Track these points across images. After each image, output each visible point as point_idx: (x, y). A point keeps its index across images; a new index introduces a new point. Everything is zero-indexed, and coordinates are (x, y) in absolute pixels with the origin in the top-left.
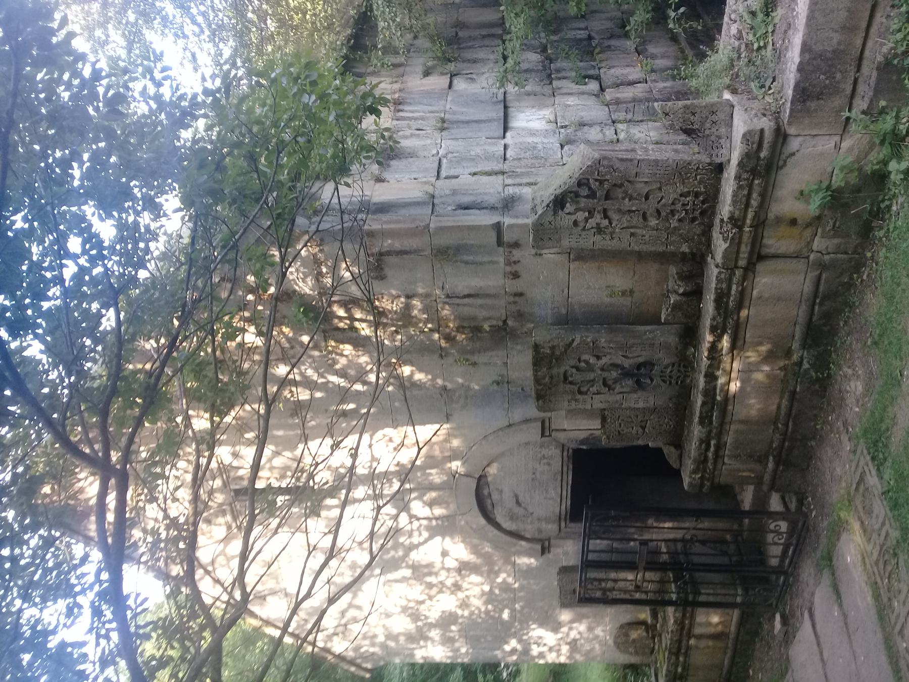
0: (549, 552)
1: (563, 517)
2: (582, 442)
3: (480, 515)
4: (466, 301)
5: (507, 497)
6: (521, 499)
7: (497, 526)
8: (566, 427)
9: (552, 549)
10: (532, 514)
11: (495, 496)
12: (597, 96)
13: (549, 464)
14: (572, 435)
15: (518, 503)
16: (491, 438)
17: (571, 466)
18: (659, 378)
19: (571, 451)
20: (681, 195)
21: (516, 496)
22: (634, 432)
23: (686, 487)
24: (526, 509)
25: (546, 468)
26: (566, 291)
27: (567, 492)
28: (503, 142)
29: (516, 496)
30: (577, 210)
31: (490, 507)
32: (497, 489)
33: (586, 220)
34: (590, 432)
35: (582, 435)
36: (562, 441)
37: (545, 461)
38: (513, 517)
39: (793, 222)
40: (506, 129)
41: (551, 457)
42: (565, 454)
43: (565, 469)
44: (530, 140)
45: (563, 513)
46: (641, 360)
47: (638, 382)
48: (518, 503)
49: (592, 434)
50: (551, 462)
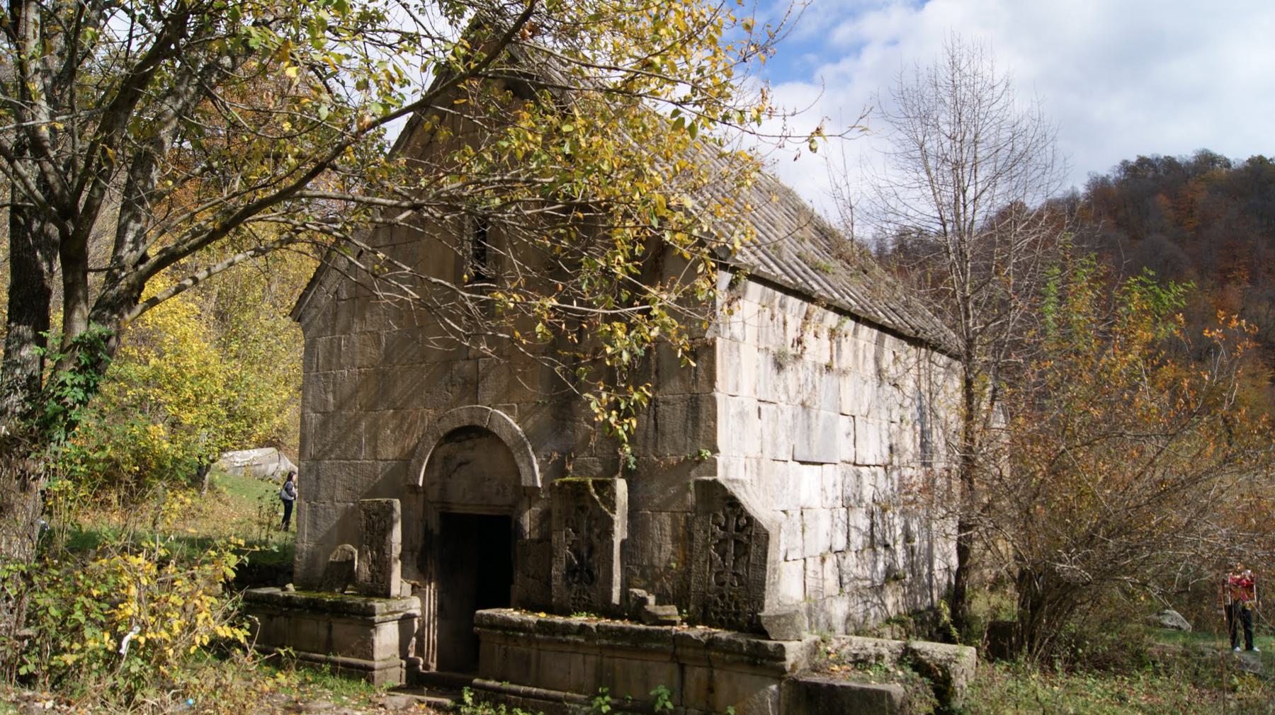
11: (468, 444)
12: (831, 548)
13: (498, 493)
15: (461, 464)
20: (737, 603)
21: (467, 463)
23: (479, 612)
27: (470, 510)
28: (789, 458)
29: (467, 463)
30: (727, 518)
33: (719, 525)
38: (447, 459)
39: (711, 690)
40: (802, 463)
44: (791, 483)
46: (595, 572)
47: (575, 570)
48: (461, 464)
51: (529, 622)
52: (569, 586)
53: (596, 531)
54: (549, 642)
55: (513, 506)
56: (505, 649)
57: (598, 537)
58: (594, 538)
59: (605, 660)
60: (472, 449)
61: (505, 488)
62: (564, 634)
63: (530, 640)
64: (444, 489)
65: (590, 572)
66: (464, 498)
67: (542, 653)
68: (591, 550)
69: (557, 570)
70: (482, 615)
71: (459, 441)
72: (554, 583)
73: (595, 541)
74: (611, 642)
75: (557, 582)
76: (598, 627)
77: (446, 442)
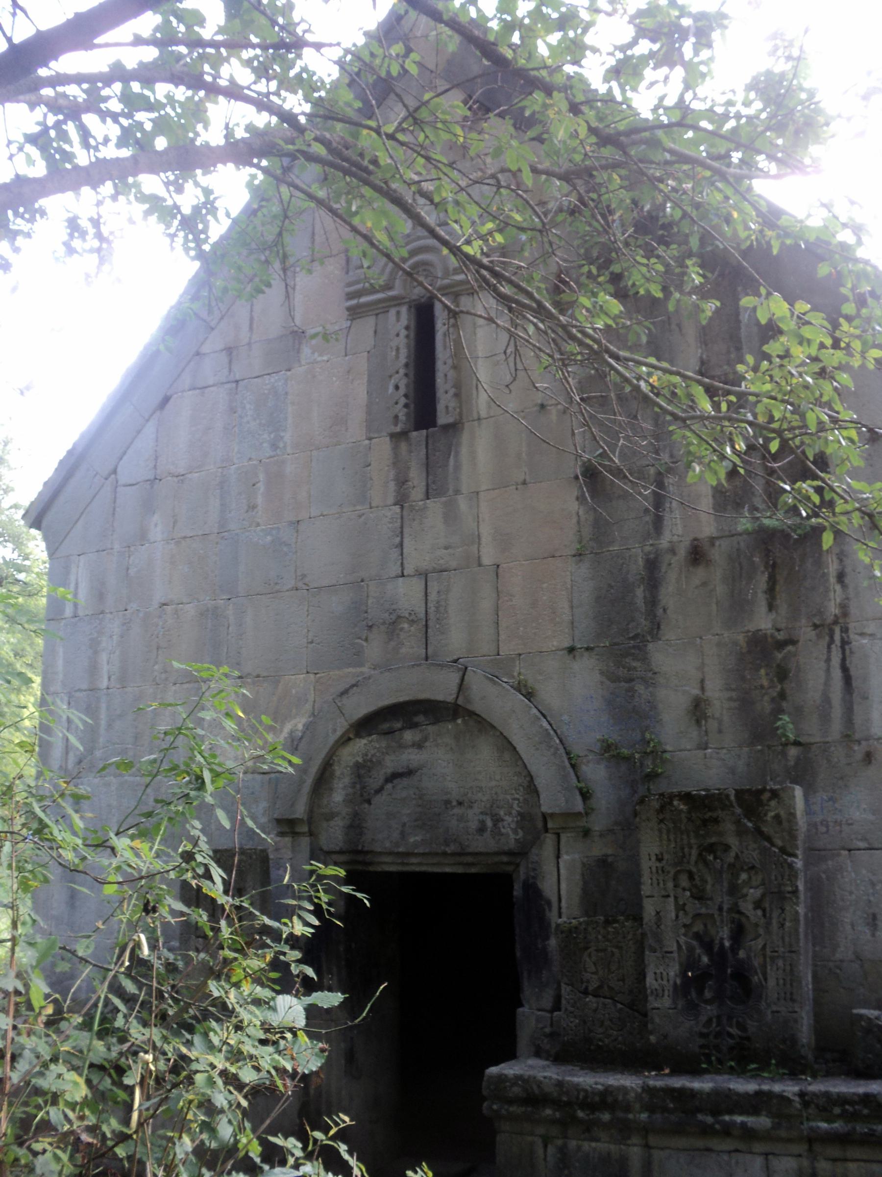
0: (282, 834)
1: (360, 858)
2: (532, 890)
3: (372, 708)
4: (837, 674)
5: (411, 757)
6: (405, 781)
7: (344, 740)
8: (565, 857)
9: (288, 840)
10: (369, 802)
11: (409, 736)
13: (482, 829)
14: (548, 867)
16: (545, 724)
17: (473, 870)
18: (715, 1012)
19: (510, 868)
22: (587, 976)
23: (493, 1070)
24: (379, 790)
25: (474, 825)
26: (862, 845)
29: (409, 773)
31: (385, 726)
32: (425, 739)
34: (554, 900)
35: (548, 887)
36: (534, 850)
37: (489, 823)
38: (362, 770)
41: (497, 832)
42: (505, 859)
43: (470, 859)
45: (369, 858)
49: (549, 903)
50: (487, 834)
51: (624, 1090)
52: (692, 1008)
53: (754, 893)
54: (678, 1130)
55: (521, 853)
56: (562, 1150)
57: (758, 905)
58: (747, 907)
59: (823, 1166)
60: (419, 745)
61: (497, 820)
62: (716, 1112)
63: (624, 1130)
64: (356, 826)
65: (742, 976)
66: (396, 836)
67: (657, 1154)
68: (739, 933)
69: (662, 974)
70: (501, 1079)
71: (390, 732)
72: (653, 1003)
73: (753, 915)
74: (838, 1125)
75: (662, 1004)
76: (802, 1094)
77: (358, 735)
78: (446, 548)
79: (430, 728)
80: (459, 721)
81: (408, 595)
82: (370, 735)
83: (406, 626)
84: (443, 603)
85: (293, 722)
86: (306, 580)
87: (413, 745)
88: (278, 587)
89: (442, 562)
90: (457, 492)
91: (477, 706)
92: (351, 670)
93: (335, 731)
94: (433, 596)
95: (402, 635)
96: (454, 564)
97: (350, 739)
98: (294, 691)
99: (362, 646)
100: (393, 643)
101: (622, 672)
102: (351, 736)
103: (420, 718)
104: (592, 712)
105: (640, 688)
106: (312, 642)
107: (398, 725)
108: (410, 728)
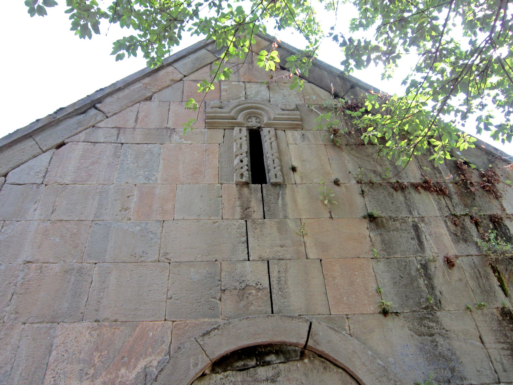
31: (240, 364)
32: (278, 375)
78: (282, 246)
79: (281, 365)
80: (306, 361)
81: (255, 273)
82: (225, 371)
83: (254, 292)
84: (283, 279)
85: (148, 359)
86: (168, 257)
87: (267, 380)
88: (143, 259)
89: (278, 254)
90: (286, 217)
91: (323, 348)
92: (206, 320)
93: (197, 364)
94: (274, 274)
95: (251, 298)
96: (288, 256)
97: (204, 375)
98: (151, 334)
99: (217, 303)
100: (243, 303)
101: (424, 330)
102: (207, 372)
103: (272, 358)
104: (410, 356)
105: (440, 340)
106: (171, 298)
107: (253, 363)
108: (263, 366)
